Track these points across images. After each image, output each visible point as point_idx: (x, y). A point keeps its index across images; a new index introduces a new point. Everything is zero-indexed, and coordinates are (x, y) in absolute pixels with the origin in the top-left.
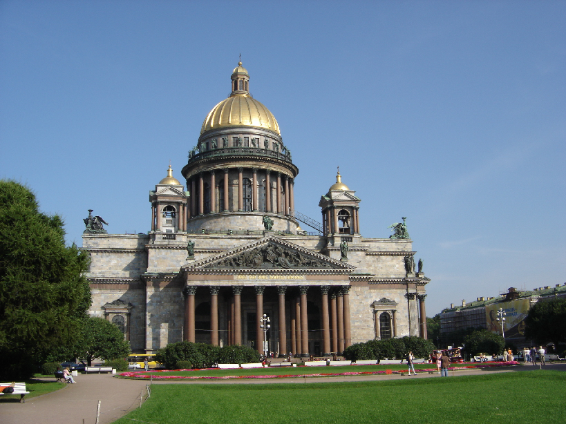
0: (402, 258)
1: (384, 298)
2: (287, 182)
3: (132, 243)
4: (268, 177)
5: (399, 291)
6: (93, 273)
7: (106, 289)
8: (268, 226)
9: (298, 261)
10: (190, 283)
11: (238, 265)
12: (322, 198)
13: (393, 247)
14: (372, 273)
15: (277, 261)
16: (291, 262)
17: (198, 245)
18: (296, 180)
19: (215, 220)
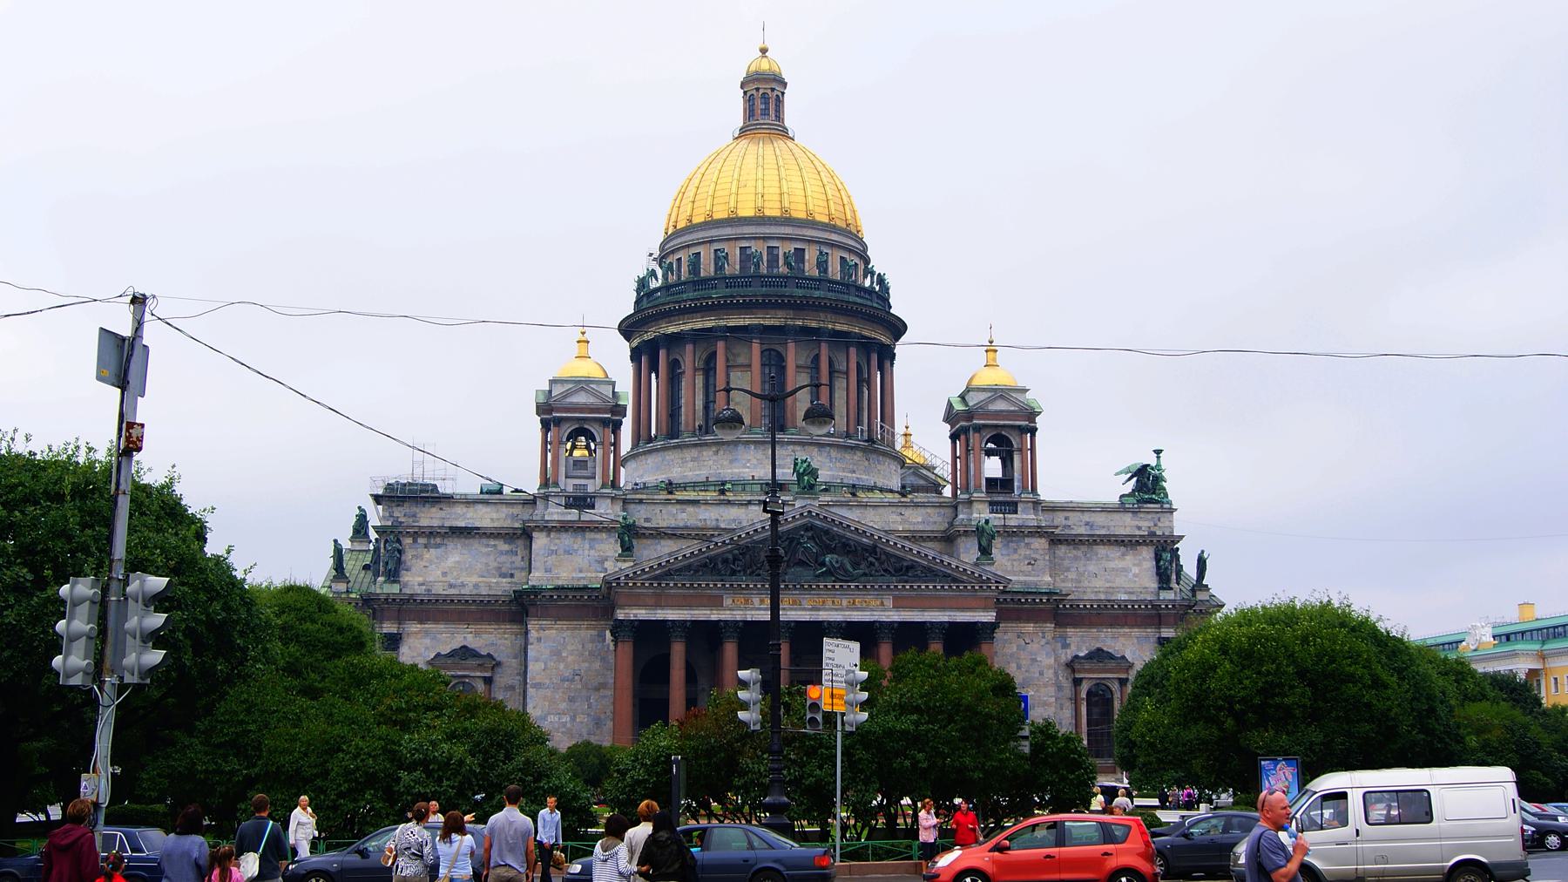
0: (1147, 554)
1: (1099, 650)
2: (875, 357)
3: (495, 516)
4: (824, 346)
5: (1136, 632)
6: (406, 585)
7: (436, 621)
8: (807, 481)
9: (872, 564)
10: (621, 615)
11: (734, 573)
12: (950, 405)
13: (1126, 525)
14: (1064, 586)
15: (823, 564)
16: (856, 565)
17: (647, 520)
18: (899, 349)
19: (694, 452)
